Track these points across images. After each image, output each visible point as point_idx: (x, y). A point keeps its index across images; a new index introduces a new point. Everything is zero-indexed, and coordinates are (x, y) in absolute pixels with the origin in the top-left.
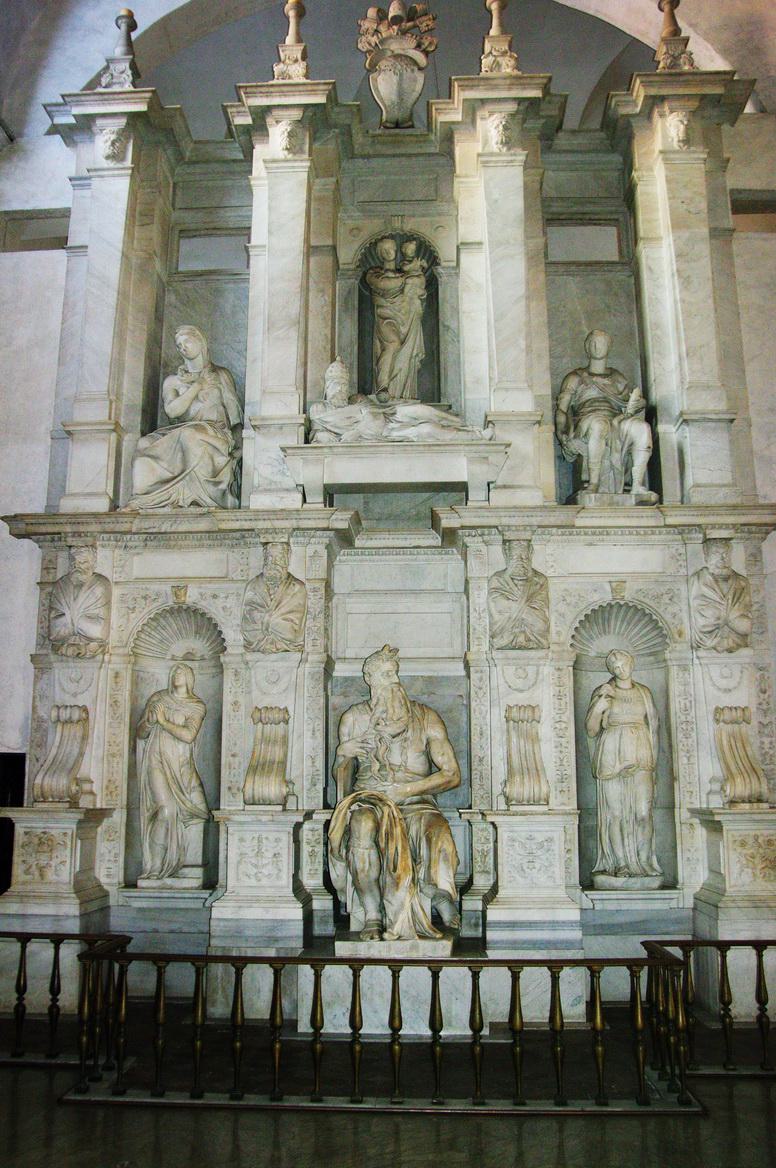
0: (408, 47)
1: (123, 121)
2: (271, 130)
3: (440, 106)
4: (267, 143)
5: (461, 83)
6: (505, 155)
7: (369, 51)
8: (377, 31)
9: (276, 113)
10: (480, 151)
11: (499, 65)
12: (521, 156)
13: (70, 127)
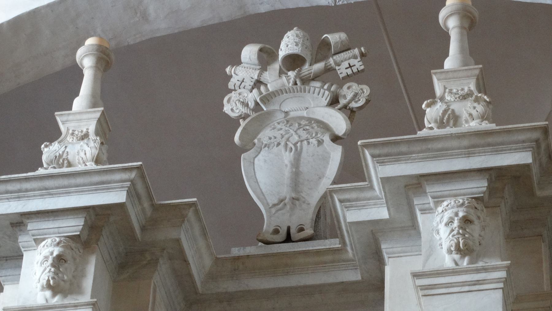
0: (315, 104)
2: (27, 257)
3: (347, 196)
5: (377, 151)
6: (466, 271)
7: (245, 117)
8: (258, 83)
9: (32, 226)
10: (418, 268)
11: (455, 119)
12: (496, 268)
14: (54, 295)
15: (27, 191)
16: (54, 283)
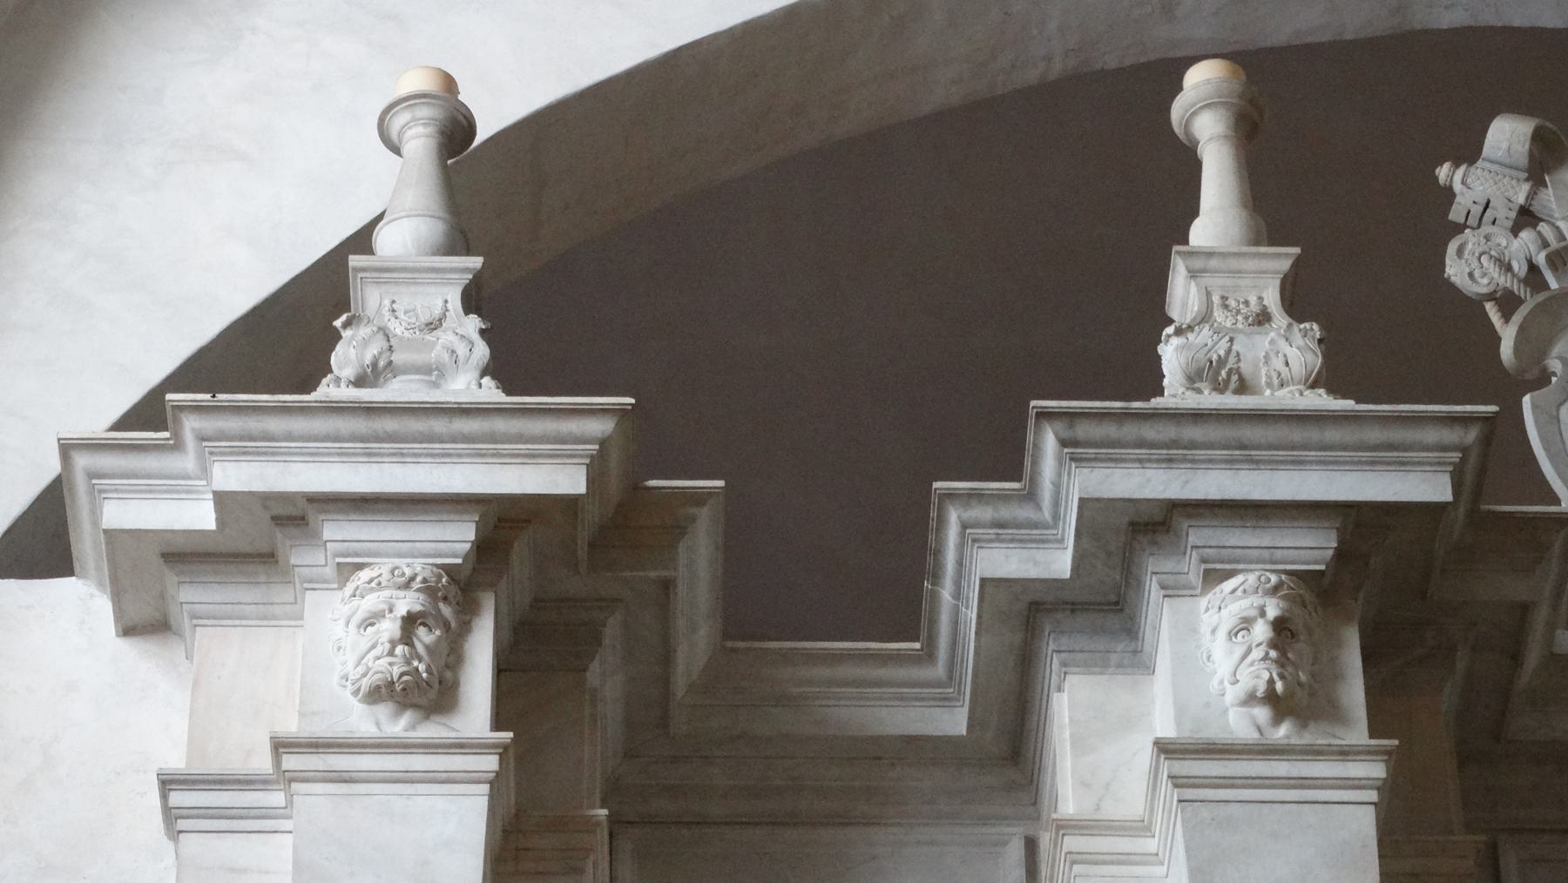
1: (459, 536)
4: (1139, 662)
8: (1526, 217)
13: (185, 555)
14: (1277, 719)
15: (1193, 445)
16: (1286, 687)
